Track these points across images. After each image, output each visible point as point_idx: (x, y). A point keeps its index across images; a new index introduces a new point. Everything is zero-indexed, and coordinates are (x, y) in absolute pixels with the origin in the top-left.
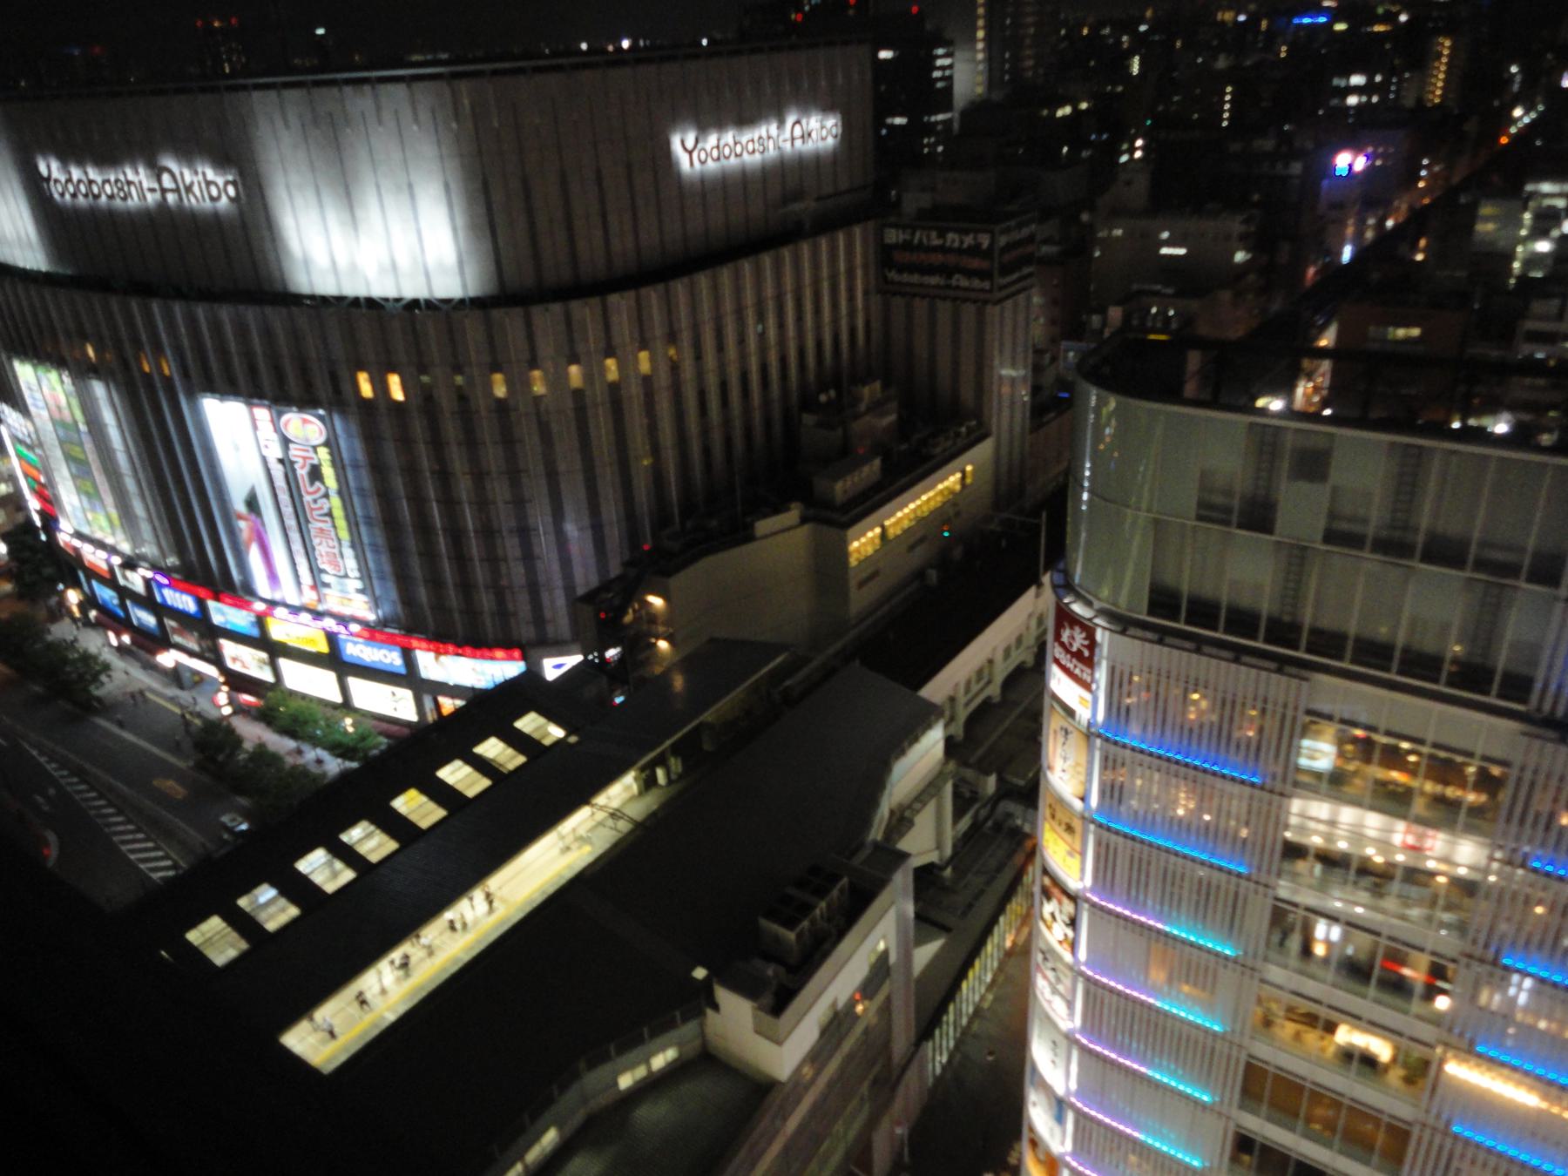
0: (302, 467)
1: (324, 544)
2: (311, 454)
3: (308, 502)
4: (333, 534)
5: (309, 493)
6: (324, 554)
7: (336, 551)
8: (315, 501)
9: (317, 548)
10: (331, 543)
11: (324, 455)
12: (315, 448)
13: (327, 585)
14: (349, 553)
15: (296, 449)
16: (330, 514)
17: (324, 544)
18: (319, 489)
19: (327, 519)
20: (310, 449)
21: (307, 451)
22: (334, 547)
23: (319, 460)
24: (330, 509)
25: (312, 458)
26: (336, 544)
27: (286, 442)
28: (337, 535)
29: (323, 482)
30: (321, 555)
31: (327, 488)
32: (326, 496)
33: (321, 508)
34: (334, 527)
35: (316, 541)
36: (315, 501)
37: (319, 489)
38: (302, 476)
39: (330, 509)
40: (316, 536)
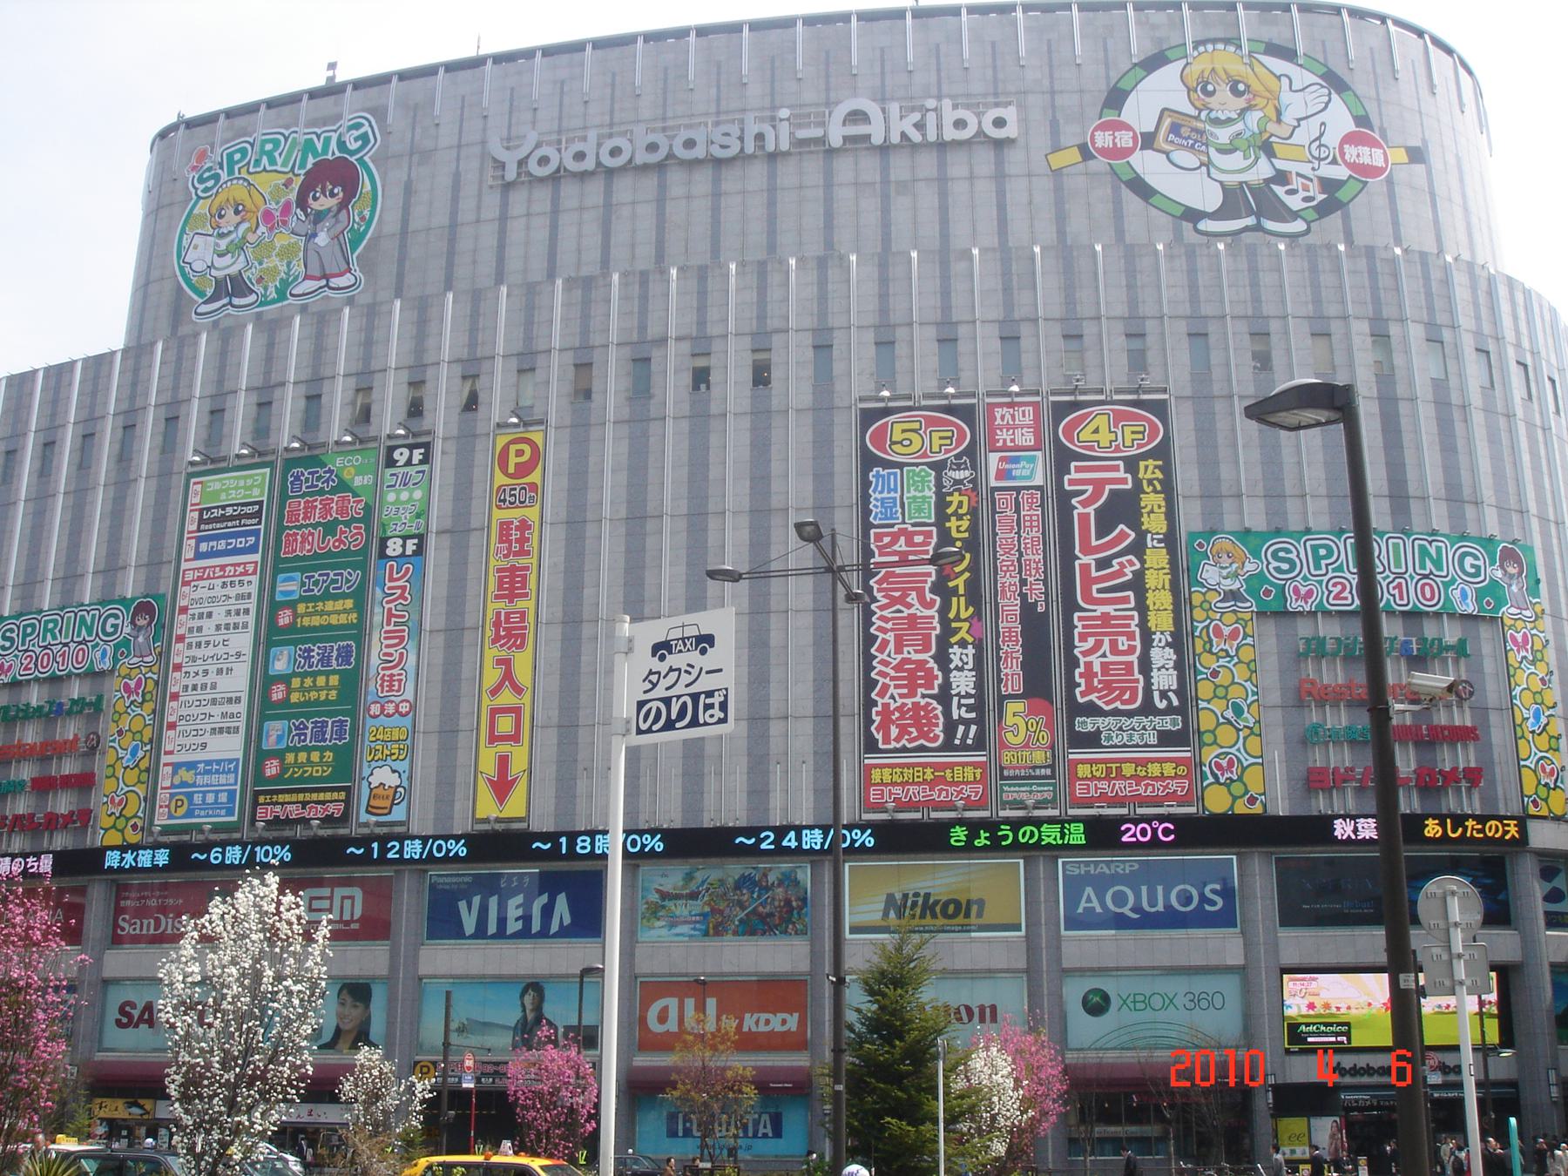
0: (1085, 504)
1: (1106, 647)
2: (1121, 474)
3: (1085, 568)
4: (1136, 621)
5: (1087, 550)
6: (1097, 668)
7: (1134, 658)
8: (1103, 564)
9: (1082, 660)
10: (1123, 643)
11: (1149, 470)
12: (1132, 464)
13: (1092, 740)
14: (1162, 656)
15: (1078, 469)
16: (1138, 585)
17: (1106, 647)
18: (1123, 536)
19: (1130, 594)
20: (1121, 463)
21: (1116, 469)
22: (1131, 650)
23: (1138, 483)
24: (1139, 576)
25: (1124, 481)
26: (1138, 643)
27: (1063, 459)
28: (1143, 623)
29: (1135, 524)
30: (1089, 674)
31: (1142, 535)
32: (1138, 549)
33: (1120, 573)
34: (1142, 608)
35: (1080, 647)
36: (1103, 564)
37: (1123, 536)
38: (1084, 518)
39: (1139, 576)
40: (1083, 638)
